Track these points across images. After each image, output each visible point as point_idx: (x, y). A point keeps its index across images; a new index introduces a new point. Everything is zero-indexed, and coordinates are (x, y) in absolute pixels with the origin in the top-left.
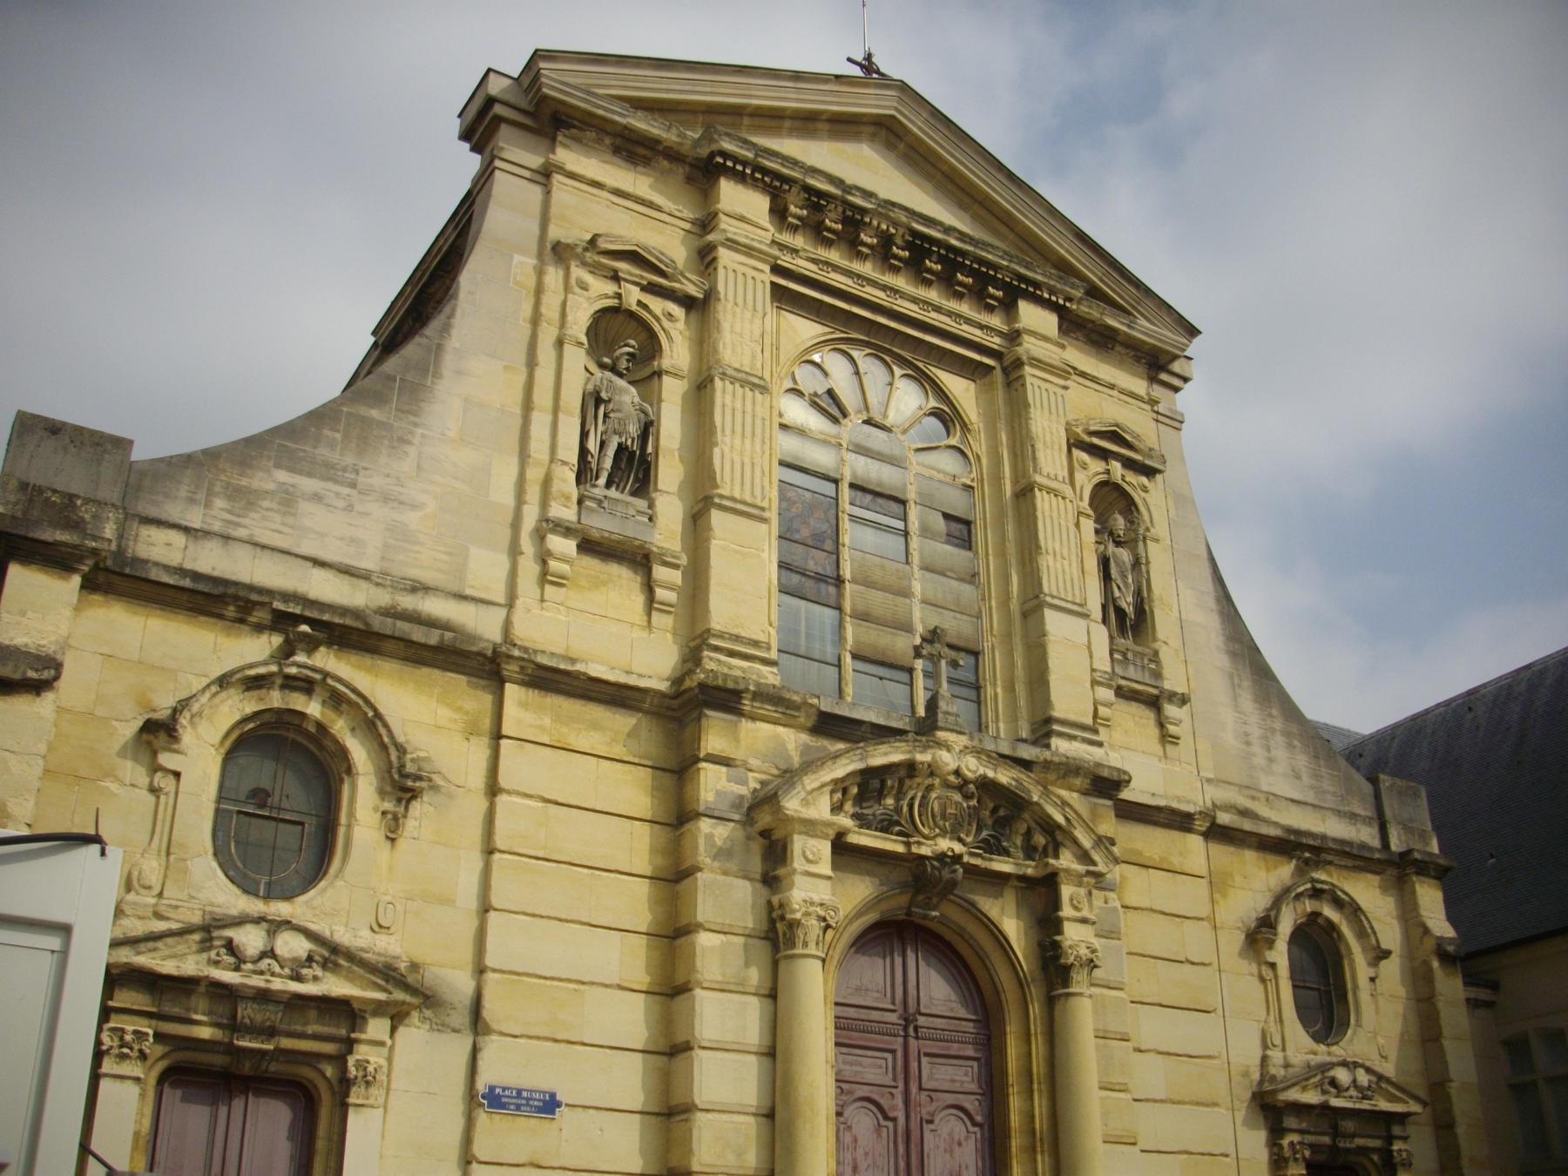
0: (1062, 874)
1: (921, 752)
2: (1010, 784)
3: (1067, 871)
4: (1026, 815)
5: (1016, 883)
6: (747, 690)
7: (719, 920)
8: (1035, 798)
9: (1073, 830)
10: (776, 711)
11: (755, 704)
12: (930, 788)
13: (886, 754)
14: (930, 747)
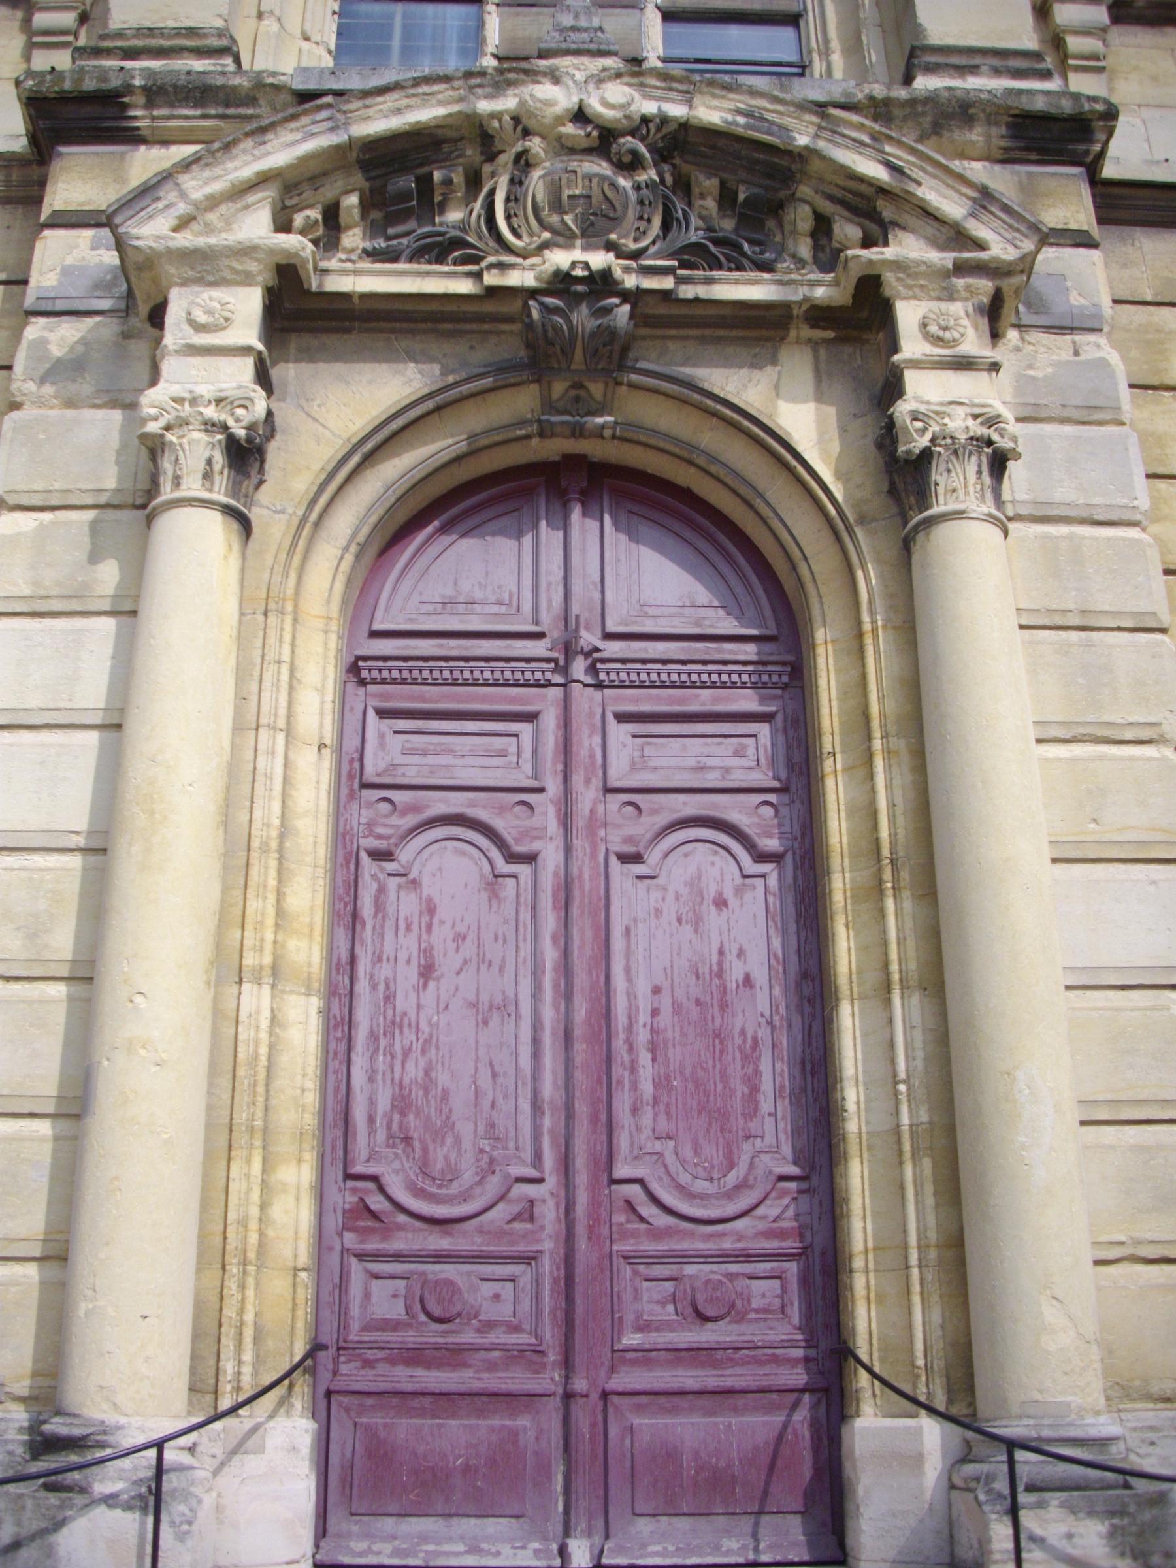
0: (889, 277)
1: (488, 97)
2: (735, 123)
3: (898, 265)
4: (805, 190)
5: (807, 332)
6: (128, 89)
7: (39, 486)
8: (802, 140)
9: (912, 187)
10: (204, 117)
11: (155, 113)
12: (524, 162)
13: (398, 111)
14: (510, 84)
